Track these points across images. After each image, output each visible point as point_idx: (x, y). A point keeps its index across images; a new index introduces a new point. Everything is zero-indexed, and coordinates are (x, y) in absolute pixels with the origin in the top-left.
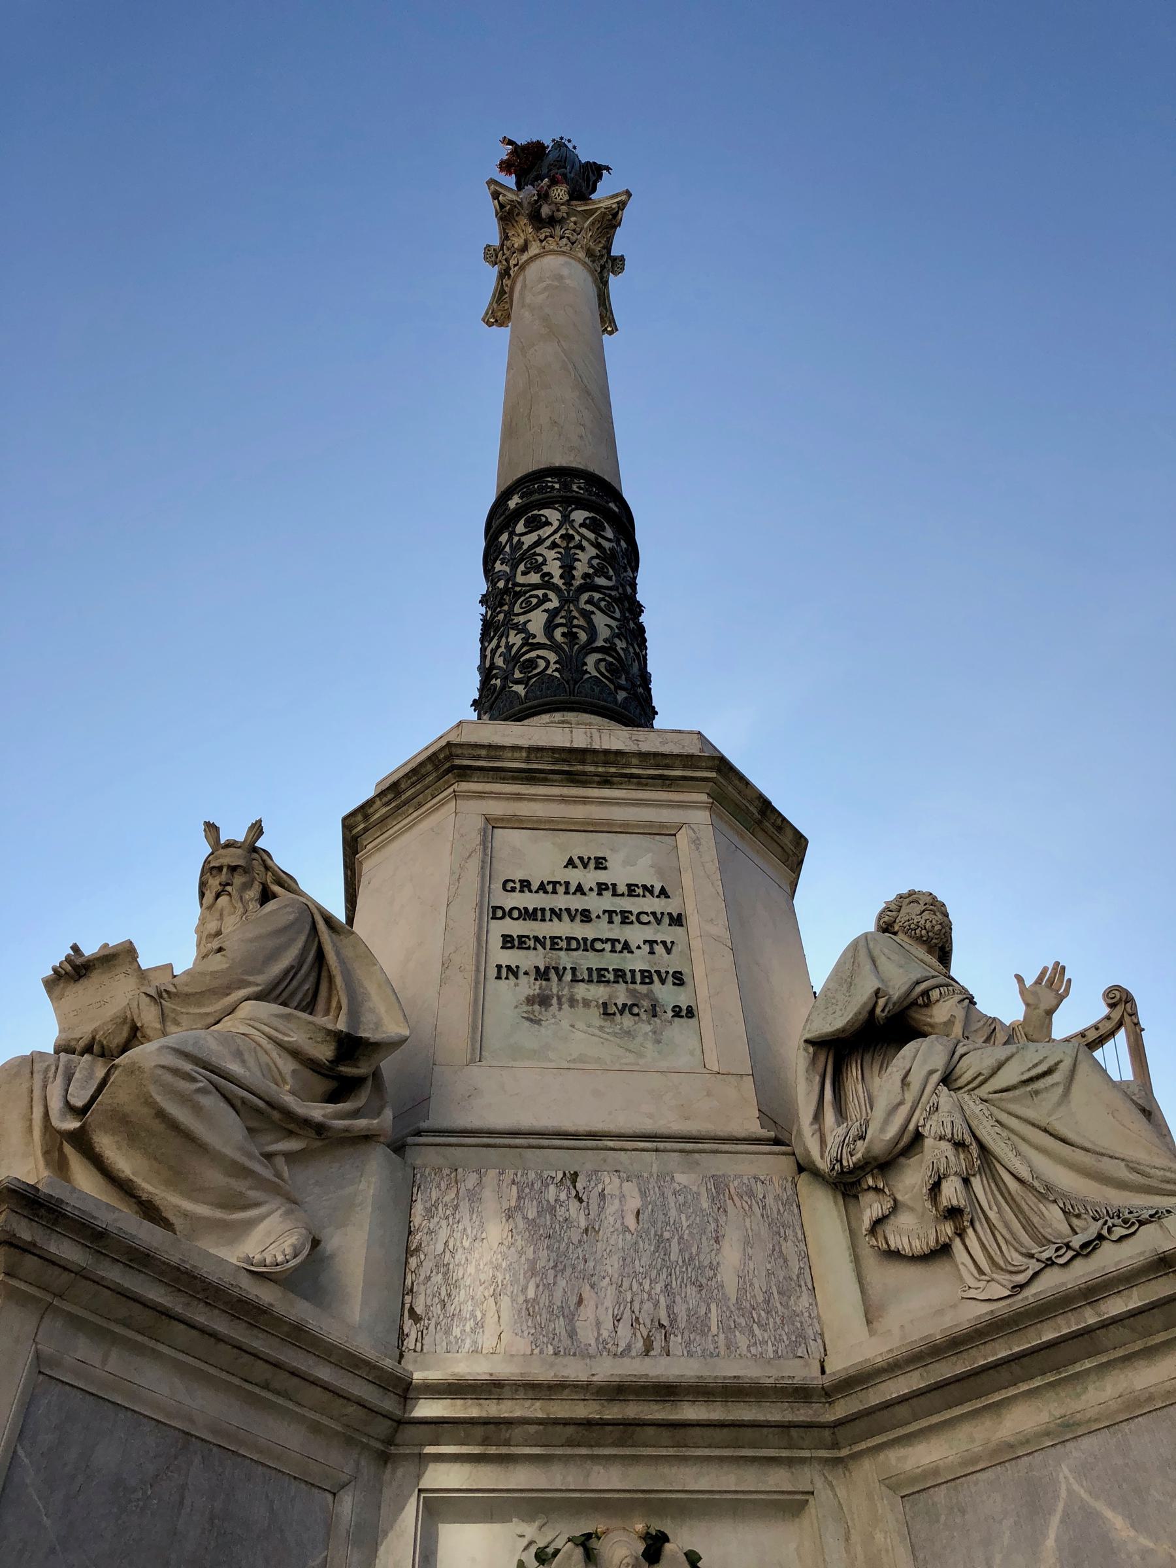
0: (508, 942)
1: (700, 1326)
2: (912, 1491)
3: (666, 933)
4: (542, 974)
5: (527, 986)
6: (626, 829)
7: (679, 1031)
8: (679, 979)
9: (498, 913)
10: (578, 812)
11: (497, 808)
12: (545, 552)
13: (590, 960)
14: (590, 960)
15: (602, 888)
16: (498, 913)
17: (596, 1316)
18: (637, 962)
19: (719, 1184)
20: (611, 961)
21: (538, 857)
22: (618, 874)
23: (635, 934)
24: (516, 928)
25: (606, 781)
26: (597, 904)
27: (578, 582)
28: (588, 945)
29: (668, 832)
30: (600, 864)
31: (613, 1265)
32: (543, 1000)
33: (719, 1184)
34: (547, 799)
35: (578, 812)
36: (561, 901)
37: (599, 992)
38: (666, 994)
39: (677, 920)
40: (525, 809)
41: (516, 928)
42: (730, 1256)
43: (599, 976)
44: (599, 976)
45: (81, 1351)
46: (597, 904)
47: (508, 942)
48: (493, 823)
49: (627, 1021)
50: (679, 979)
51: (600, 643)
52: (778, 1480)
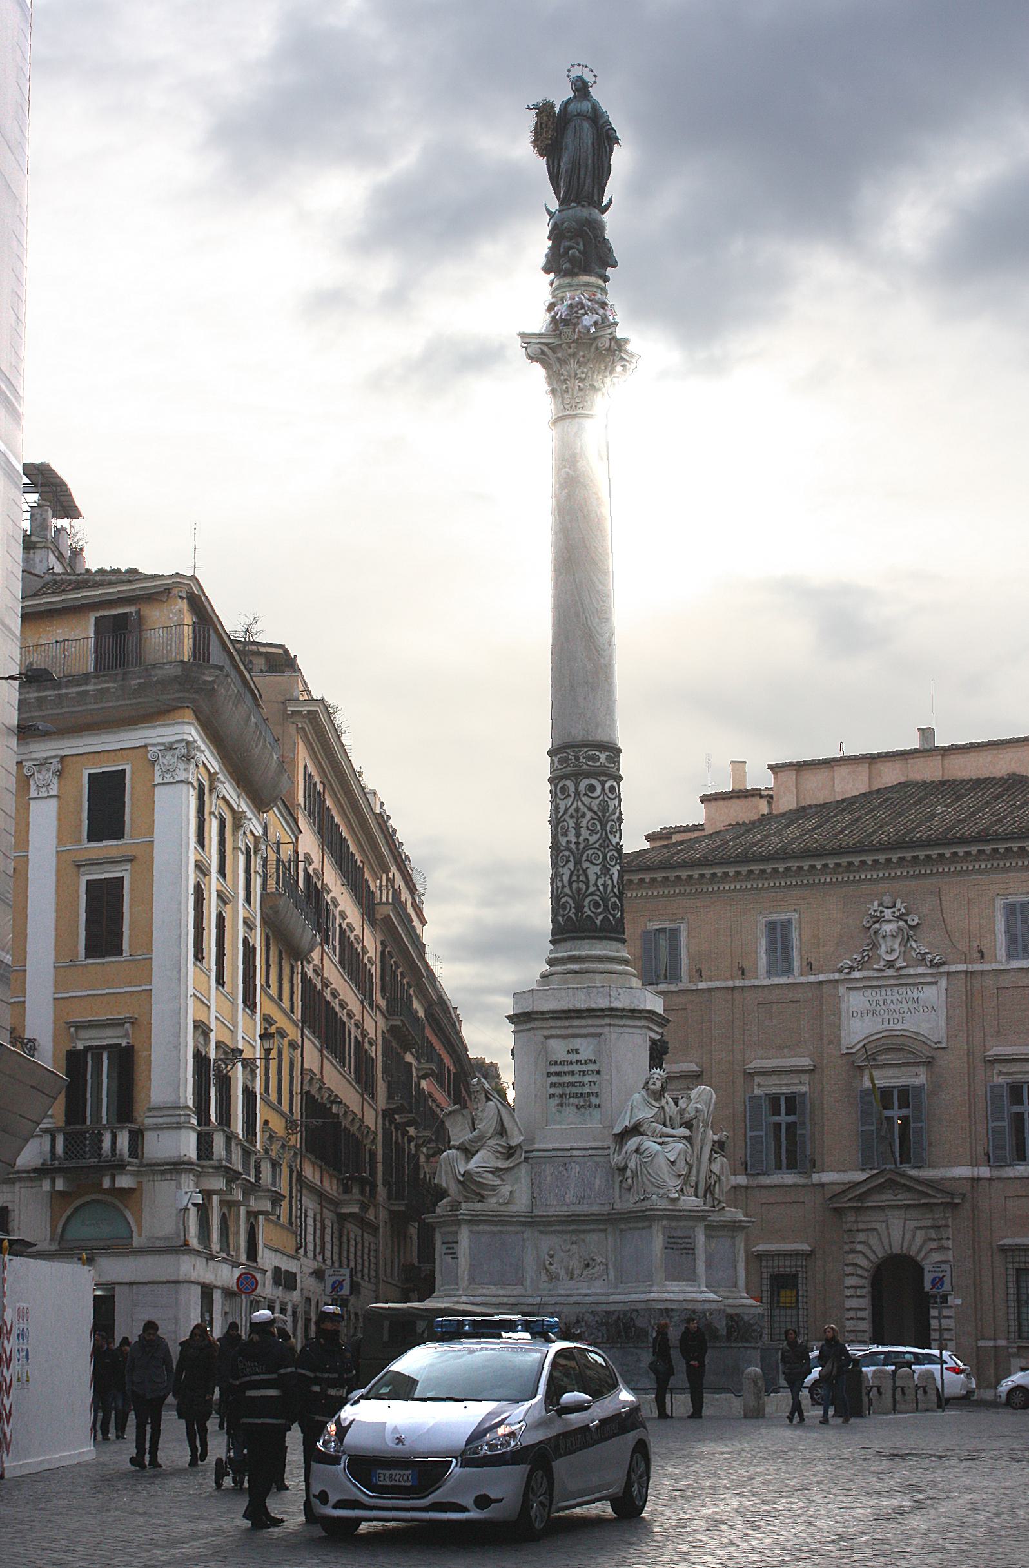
0: (552, 1085)
1: (590, 1197)
2: (622, 1230)
3: (595, 1078)
4: (561, 1096)
5: (557, 1101)
6: (585, 1036)
7: (596, 1113)
8: (597, 1095)
9: (549, 1074)
10: (570, 1031)
11: (546, 1033)
12: (568, 819)
13: (574, 1090)
14: (574, 1090)
15: (577, 1061)
16: (549, 1074)
17: (569, 1197)
18: (586, 1090)
19: (597, 1164)
20: (579, 1090)
21: (559, 1049)
22: (583, 1056)
23: (586, 1079)
24: (554, 1079)
25: (578, 1018)
26: (577, 1068)
27: (582, 846)
28: (573, 1084)
29: (600, 1035)
30: (577, 1051)
31: (573, 1185)
32: (561, 1105)
33: (597, 1164)
34: (561, 1027)
35: (570, 1031)
36: (566, 1069)
37: (576, 1101)
38: (594, 1101)
39: (598, 1072)
40: (554, 1032)
41: (554, 1079)
42: (597, 1182)
43: (576, 1096)
44: (576, 1096)
45: (475, 1227)
46: (577, 1068)
47: (552, 1085)
48: (547, 1037)
49: (583, 1110)
50: (597, 1095)
51: (592, 889)
52: (602, 1227)
